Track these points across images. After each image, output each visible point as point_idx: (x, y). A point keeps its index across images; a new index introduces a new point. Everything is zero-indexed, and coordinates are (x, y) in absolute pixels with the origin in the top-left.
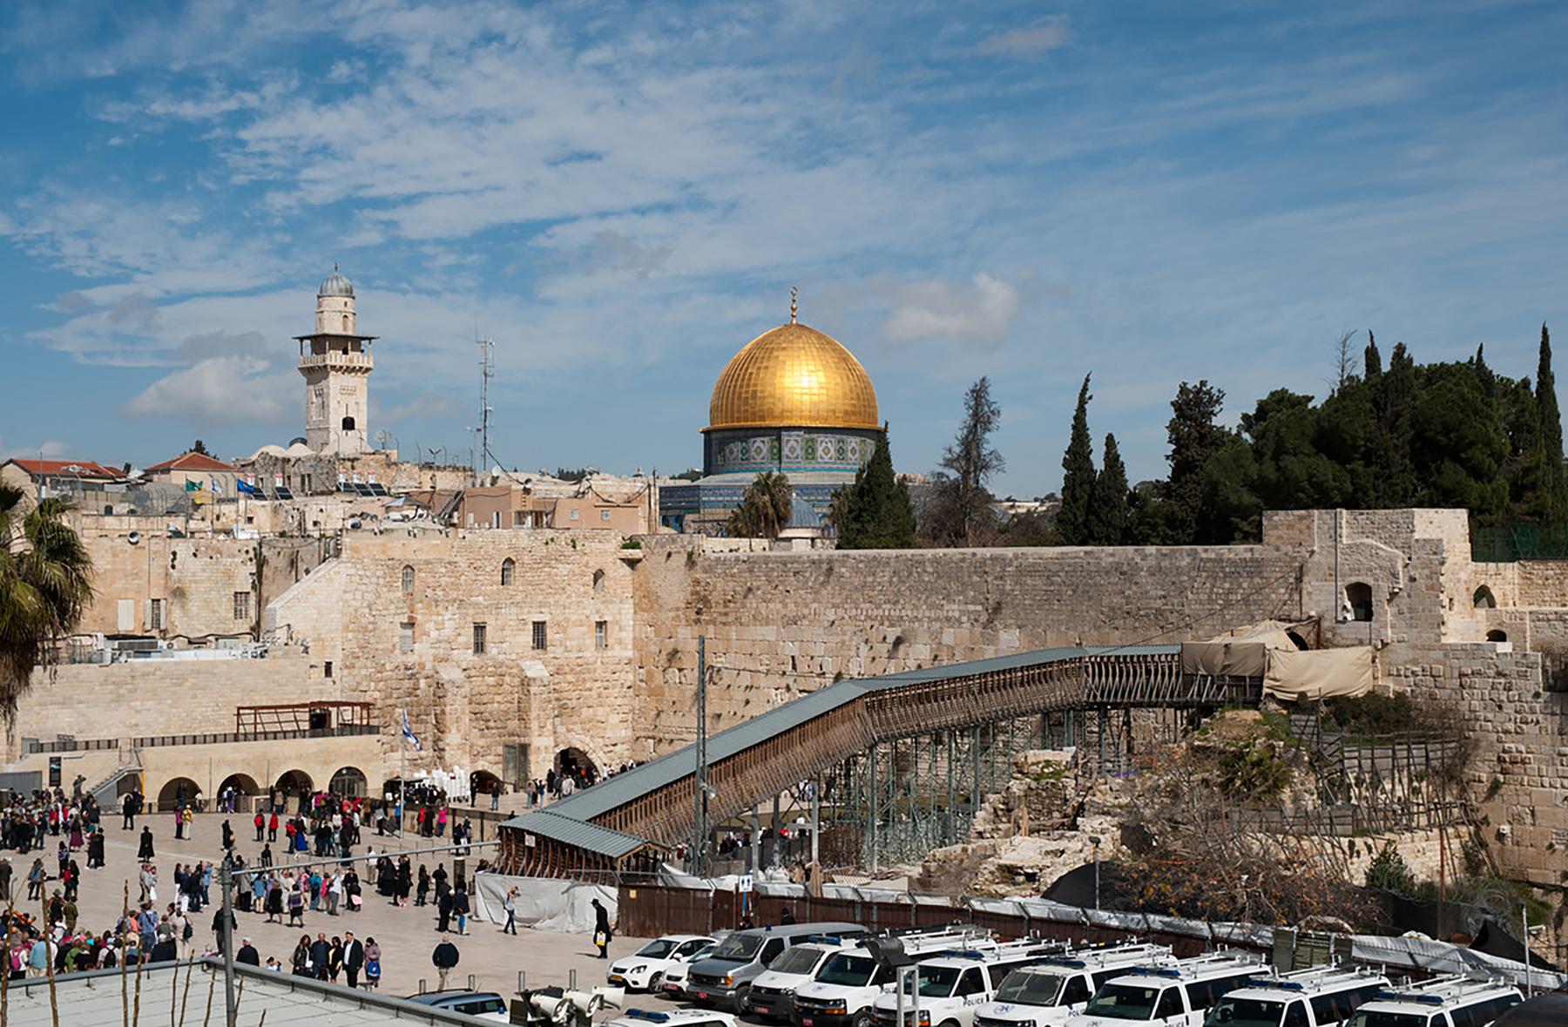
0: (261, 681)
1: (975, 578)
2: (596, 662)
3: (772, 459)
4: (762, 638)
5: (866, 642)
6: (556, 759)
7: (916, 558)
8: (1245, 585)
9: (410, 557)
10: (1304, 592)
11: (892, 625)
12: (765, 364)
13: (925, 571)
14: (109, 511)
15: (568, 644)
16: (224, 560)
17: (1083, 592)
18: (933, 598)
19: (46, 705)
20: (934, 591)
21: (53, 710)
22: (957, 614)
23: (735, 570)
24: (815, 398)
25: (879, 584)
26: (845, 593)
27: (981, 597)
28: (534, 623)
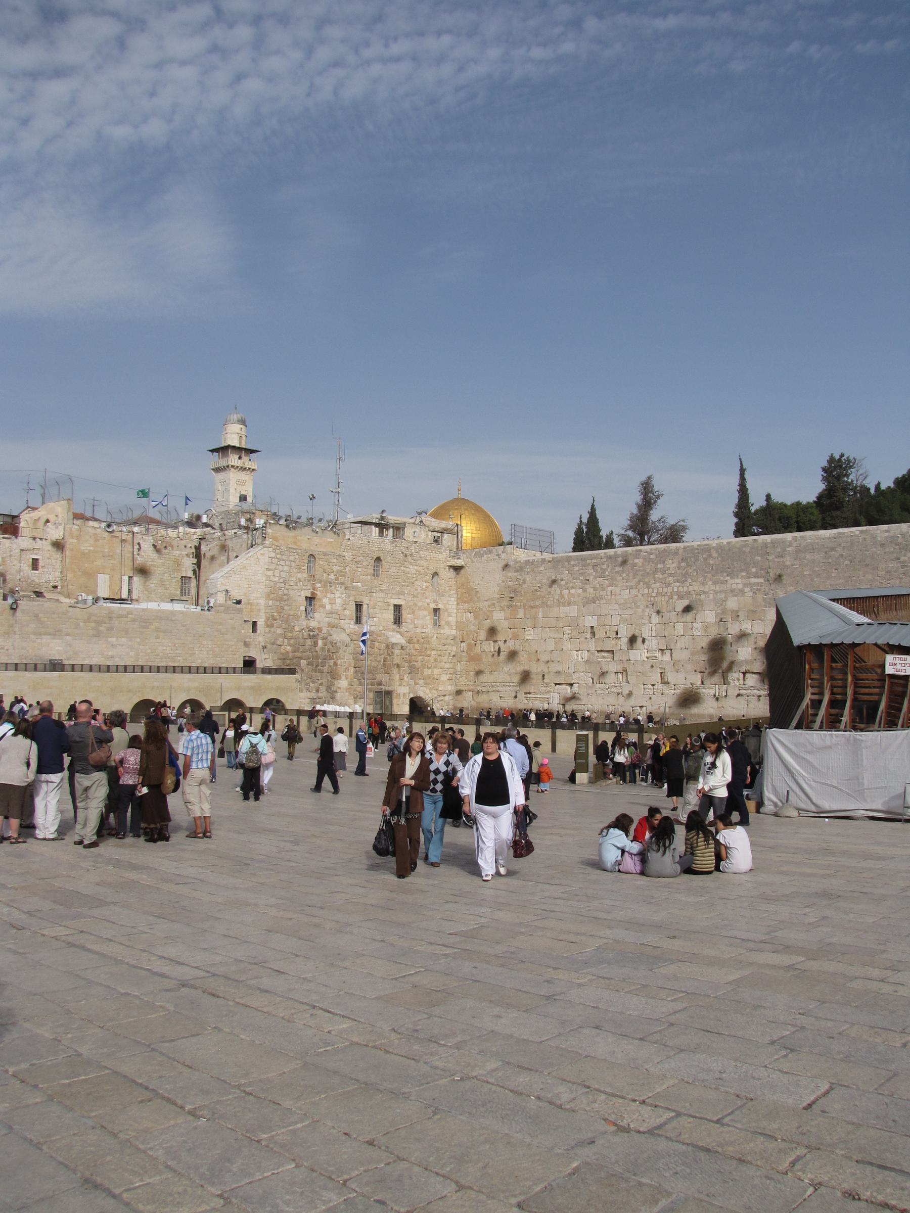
0: (208, 629)
2: (432, 637)
5: (658, 612)
7: (702, 548)
9: (314, 549)
11: (681, 597)
13: (710, 556)
16: (175, 552)
19: (40, 634)
21: (46, 639)
22: (740, 586)
24: (474, 535)
25: (669, 569)
26: (639, 577)
27: (762, 572)
28: (395, 605)
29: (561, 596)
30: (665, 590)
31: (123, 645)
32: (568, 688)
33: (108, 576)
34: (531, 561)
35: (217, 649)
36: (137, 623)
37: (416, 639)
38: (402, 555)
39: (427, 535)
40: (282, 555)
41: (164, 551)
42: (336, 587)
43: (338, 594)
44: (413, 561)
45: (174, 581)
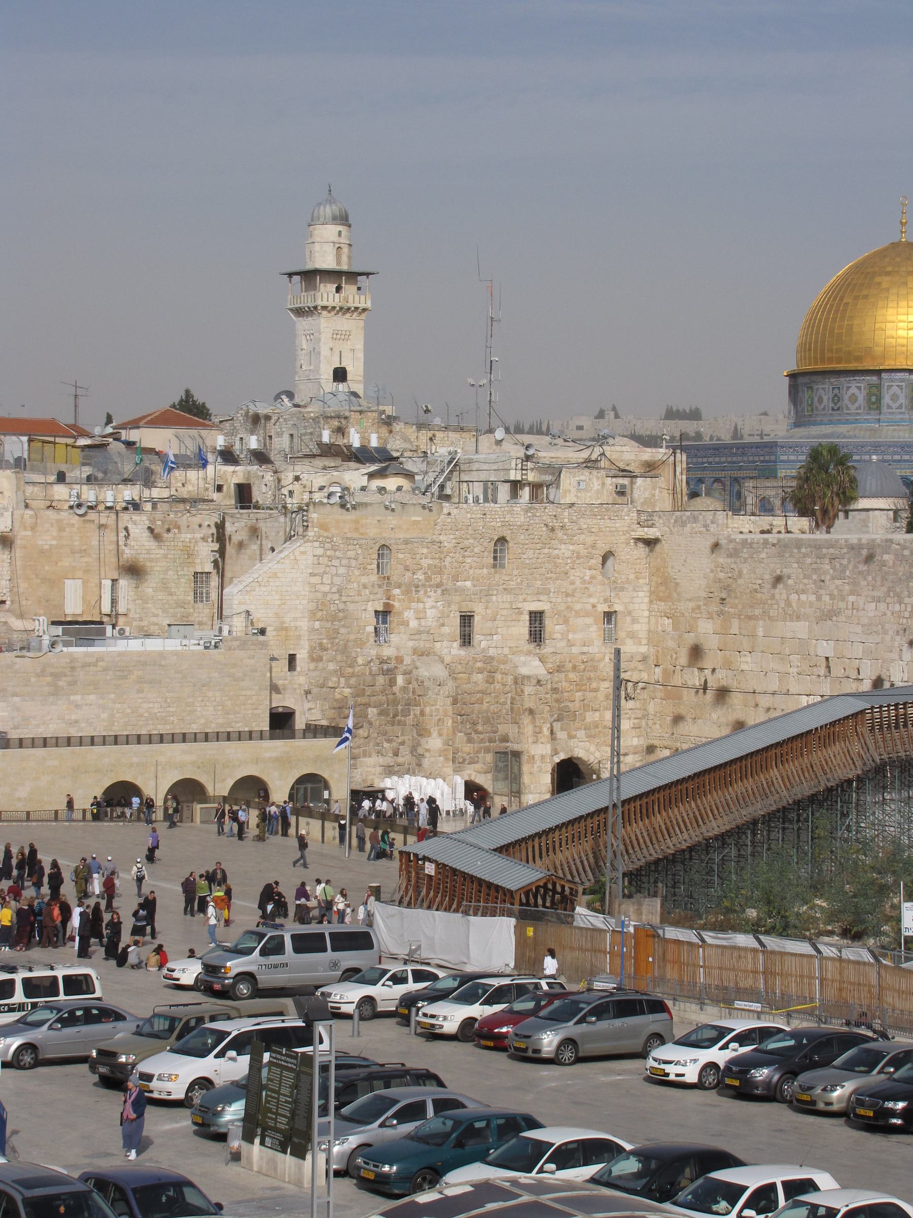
0: (216, 675)
3: (870, 409)
4: (789, 635)
6: (553, 770)
12: (865, 292)
14: (61, 478)
15: (570, 636)
16: (183, 535)
28: (531, 613)
29: (788, 603)
31: (91, 705)
33: (80, 582)
34: (749, 541)
35: (228, 703)
36: (111, 673)
37: (571, 665)
38: (544, 529)
39: (603, 484)
40: (335, 551)
41: (166, 535)
42: (426, 592)
43: (429, 602)
44: (565, 537)
45: (183, 580)
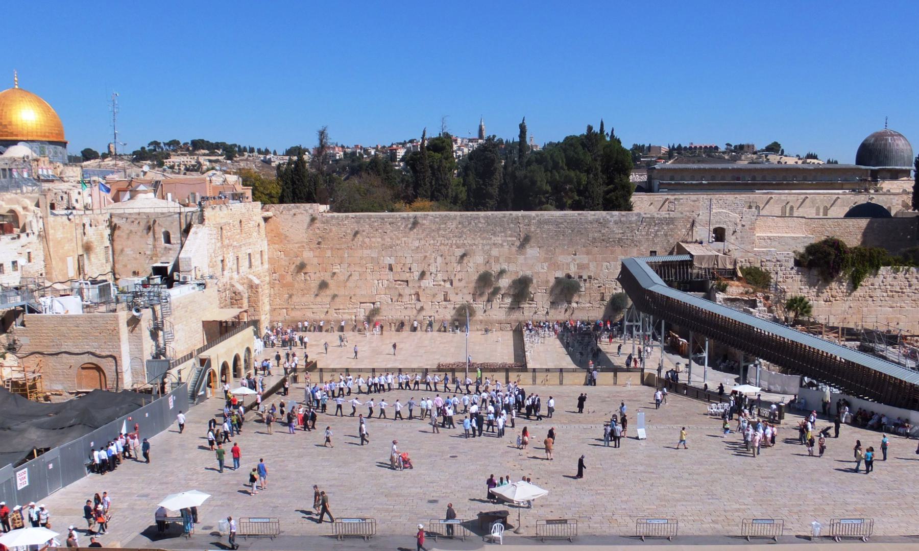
1: (512, 225)
5: (442, 256)
8: (665, 228)
10: (694, 231)
17: (578, 231)
18: (485, 235)
20: (482, 231)
22: (500, 242)
23: (346, 222)
27: (515, 234)
28: (250, 254)
29: (363, 242)
30: (447, 242)
32: (372, 305)
